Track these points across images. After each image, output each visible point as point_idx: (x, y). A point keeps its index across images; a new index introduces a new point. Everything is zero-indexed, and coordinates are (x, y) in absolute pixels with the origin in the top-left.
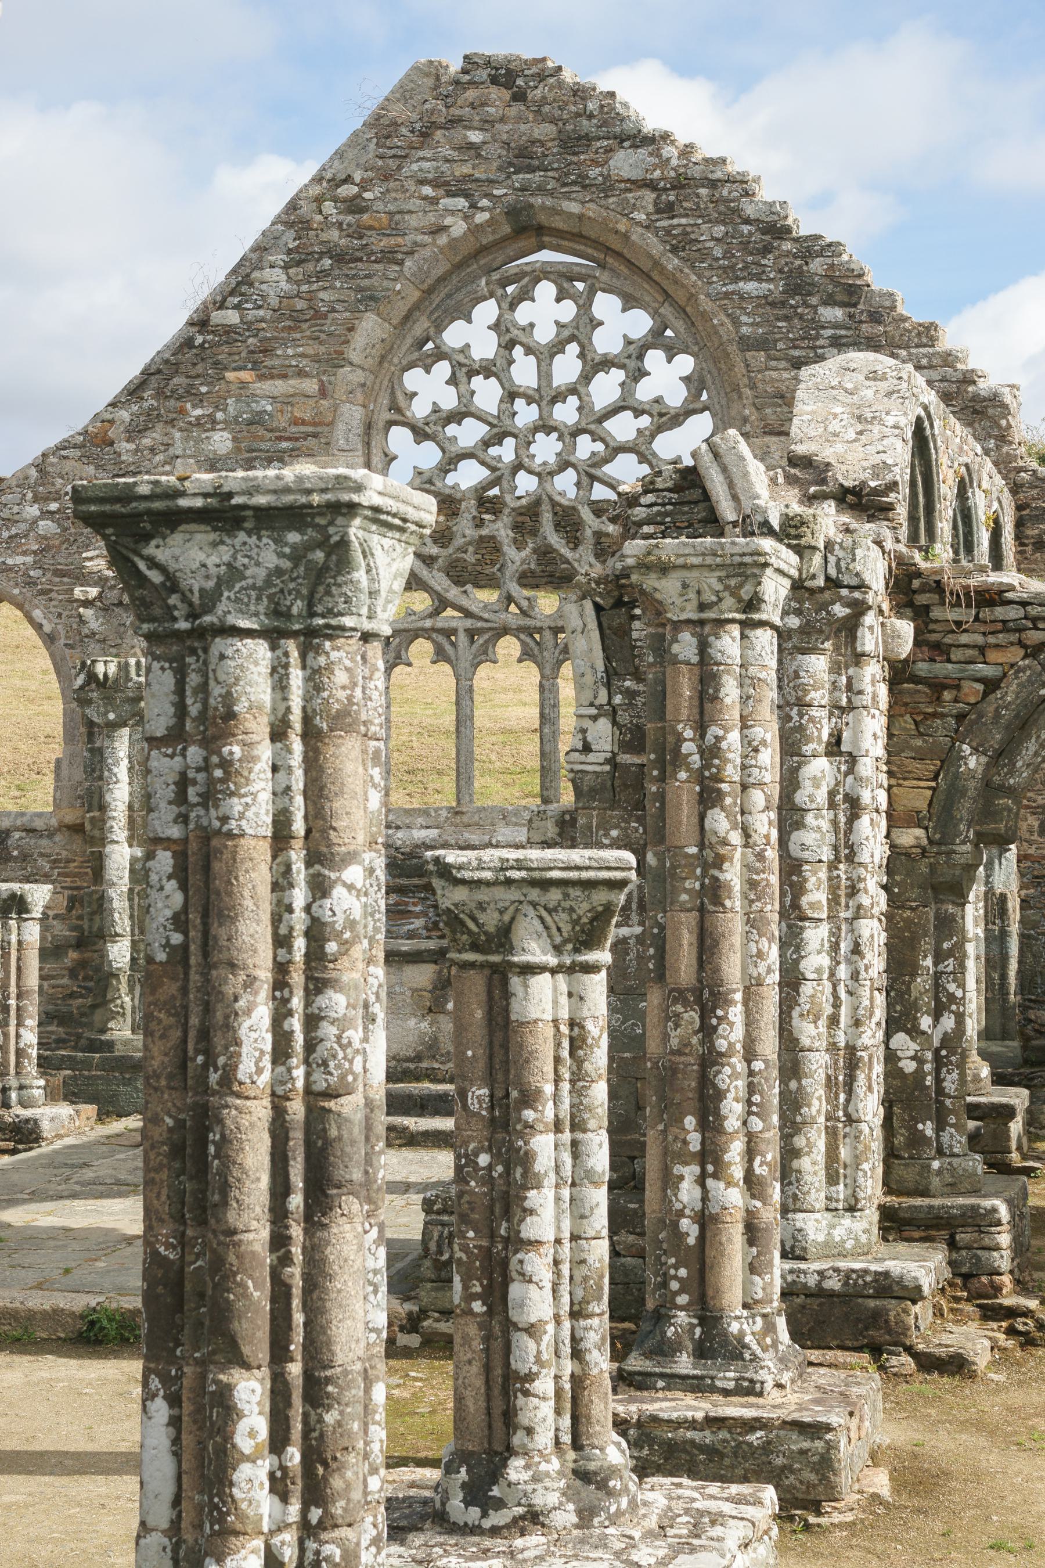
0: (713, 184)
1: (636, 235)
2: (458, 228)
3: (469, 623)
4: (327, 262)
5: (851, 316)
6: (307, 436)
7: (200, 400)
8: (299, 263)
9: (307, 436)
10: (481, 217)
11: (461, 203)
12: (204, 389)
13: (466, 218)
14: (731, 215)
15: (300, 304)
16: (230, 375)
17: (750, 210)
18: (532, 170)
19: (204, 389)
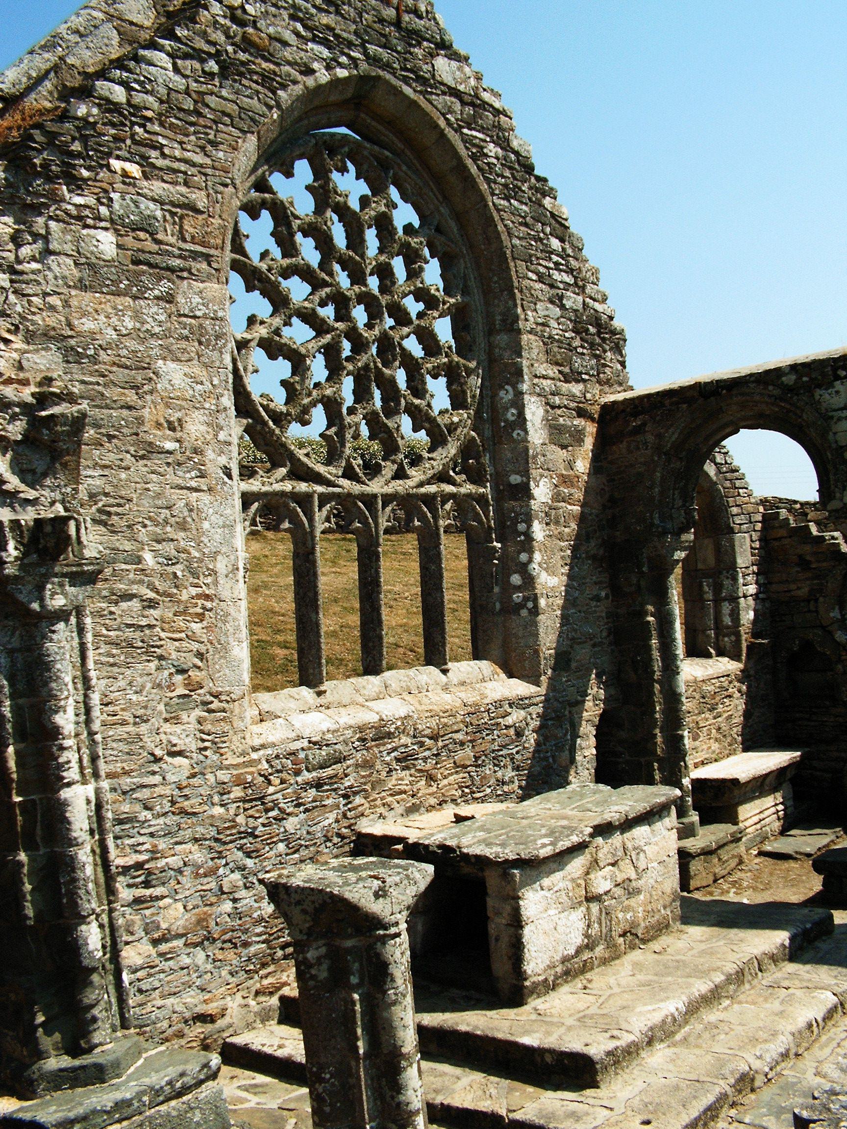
0: (497, 112)
1: (450, 133)
2: (323, 77)
3: (320, 489)
4: (212, 66)
5: (564, 249)
6: (195, 255)
7: (77, 184)
8: (186, 56)
9: (195, 255)
10: (342, 73)
11: (326, 53)
12: (85, 173)
13: (328, 68)
14: (504, 143)
15: (189, 104)
16: (116, 164)
17: (515, 144)
18: (384, 47)
19: (85, 173)
